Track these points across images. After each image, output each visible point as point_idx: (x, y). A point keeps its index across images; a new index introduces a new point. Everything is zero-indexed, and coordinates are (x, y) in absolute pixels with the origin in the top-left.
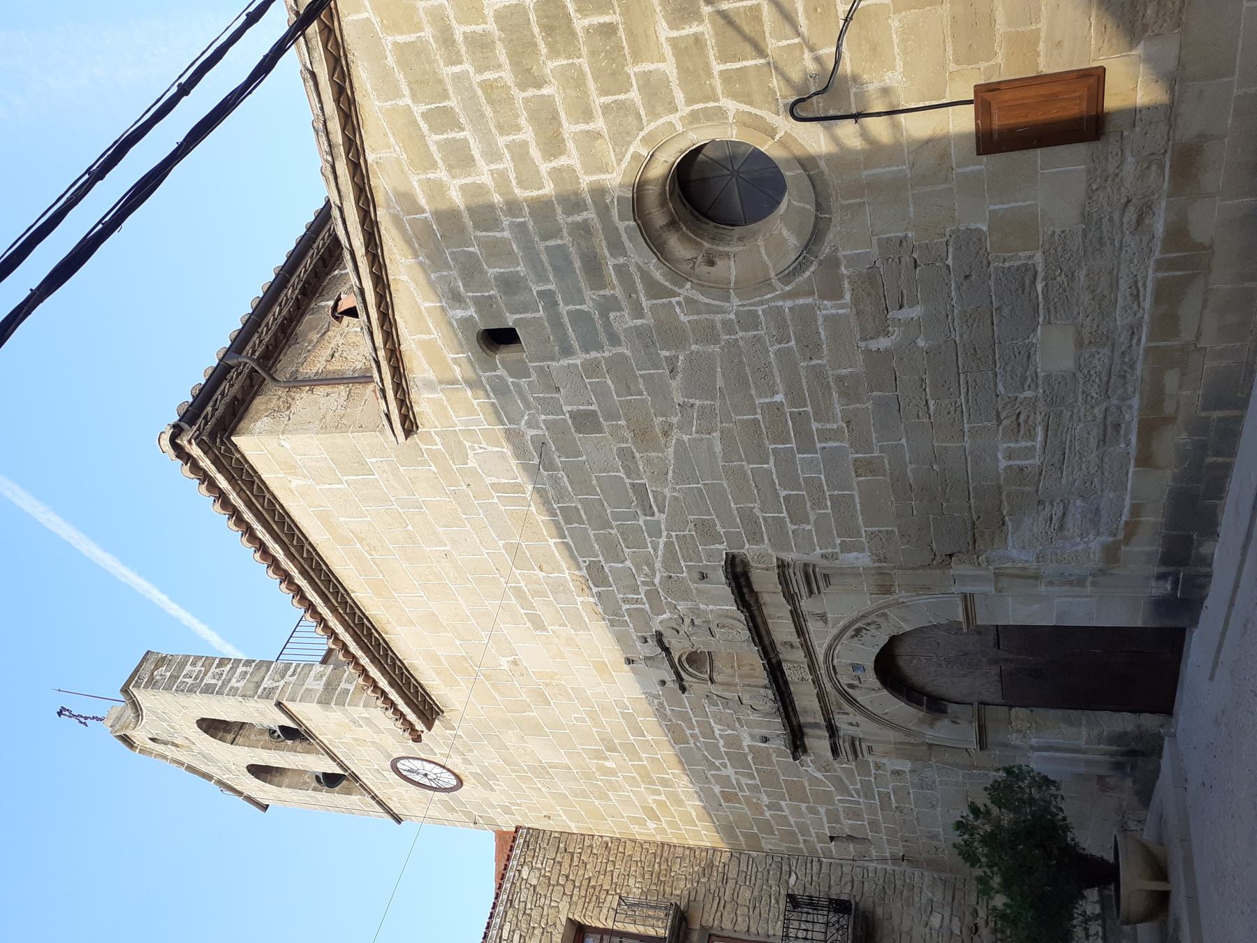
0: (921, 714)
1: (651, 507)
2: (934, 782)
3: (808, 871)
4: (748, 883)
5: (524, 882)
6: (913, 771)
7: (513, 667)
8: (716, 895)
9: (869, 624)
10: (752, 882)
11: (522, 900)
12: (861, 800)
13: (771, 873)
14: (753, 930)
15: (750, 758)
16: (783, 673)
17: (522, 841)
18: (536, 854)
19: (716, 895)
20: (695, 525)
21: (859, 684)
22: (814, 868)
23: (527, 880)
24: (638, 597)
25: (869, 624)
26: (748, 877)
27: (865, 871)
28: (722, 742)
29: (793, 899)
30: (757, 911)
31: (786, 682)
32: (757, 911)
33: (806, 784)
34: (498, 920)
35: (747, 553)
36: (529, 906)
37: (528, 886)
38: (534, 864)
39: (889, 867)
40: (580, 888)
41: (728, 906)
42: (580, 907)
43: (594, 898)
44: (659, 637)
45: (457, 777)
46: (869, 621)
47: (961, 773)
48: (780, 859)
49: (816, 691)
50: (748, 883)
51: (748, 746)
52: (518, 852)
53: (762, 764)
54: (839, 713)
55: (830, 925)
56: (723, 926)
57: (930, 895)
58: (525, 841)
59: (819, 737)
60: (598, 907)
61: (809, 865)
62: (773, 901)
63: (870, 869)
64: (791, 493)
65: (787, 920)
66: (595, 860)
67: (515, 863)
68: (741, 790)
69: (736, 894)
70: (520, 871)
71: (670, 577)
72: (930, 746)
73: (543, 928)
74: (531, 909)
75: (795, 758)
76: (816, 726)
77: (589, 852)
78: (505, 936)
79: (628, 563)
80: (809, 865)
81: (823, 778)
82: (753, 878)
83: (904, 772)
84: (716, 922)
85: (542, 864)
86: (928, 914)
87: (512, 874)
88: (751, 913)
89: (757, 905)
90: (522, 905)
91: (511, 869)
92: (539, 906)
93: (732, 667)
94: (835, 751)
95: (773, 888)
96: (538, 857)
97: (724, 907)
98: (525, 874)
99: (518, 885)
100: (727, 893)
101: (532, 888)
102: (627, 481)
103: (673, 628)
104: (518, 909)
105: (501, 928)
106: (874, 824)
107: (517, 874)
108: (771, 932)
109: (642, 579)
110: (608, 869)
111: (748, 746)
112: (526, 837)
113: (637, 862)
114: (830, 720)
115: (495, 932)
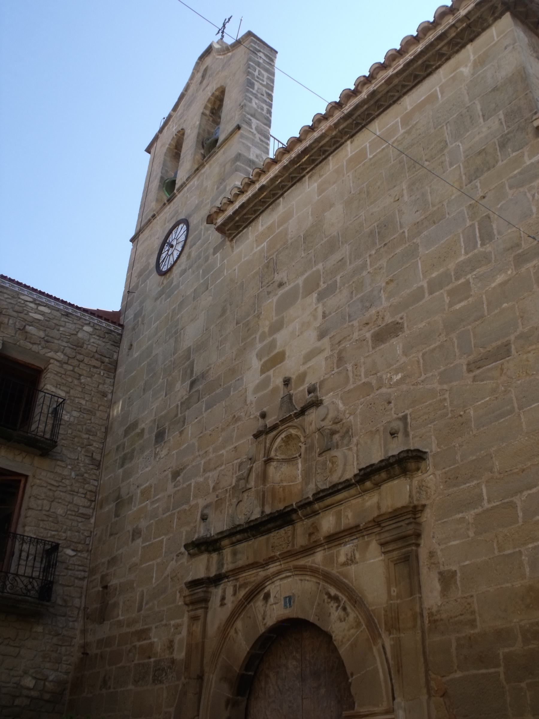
0: (237, 669)
1: (479, 368)
2: (161, 682)
3: (76, 567)
4: (69, 512)
5: (80, 327)
6: (173, 661)
7: (276, 284)
8: (61, 484)
9: (344, 609)
10: (70, 517)
11: (67, 324)
12: (142, 612)
13: (77, 534)
14: (30, 513)
15: (186, 507)
16: (280, 527)
17: (112, 328)
18: (101, 339)
19: (61, 484)
20: (461, 416)
21: (269, 603)
22: (79, 573)
23: (82, 329)
24: (363, 376)
25: (344, 609)
26: (74, 513)
27: (74, 619)
28: (201, 479)
29: (55, 547)
30: (45, 518)
31: (269, 531)
32: (45, 518)
33: (159, 560)
34: (53, 304)
35: (429, 473)
36: (62, 329)
37: (77, 330)
38: (94, 336)
39: (78, 641)
40: (73, 371)
41: (51, 494)
42: (58, 370)
43: (64, 382)
44: (316, 403)
45: (170, 270)
46: (349, 610)
47: (172, 710)
48: (87, 542)
49: (261, 561)
50: (69, 512)
51: (197, 504)
52: (104, 325)
53: (179, 519)
54: (235, 586)
55: (31, 580)
56: (34, 487)
57: (51, 678)
58: (111, 330)
59: (208, 568)
60: (57, 384)
61: (81, 568)
62: (53, 533)
63: (76, 624)
64: (519, 509)
65: (38, 541)
66: (94, 385)
67: (96, 322)
68: (153, 503)
69: (60, 501)
70: (89, 324)
71: (390, 403)
72: (200, 678)
73: (43, 338)
74: (58, 330)
75: (186, 546)
76: (221, 564)
77: (101, 381)
78: (41, 308)
79: (404, 359)
80: (81, 568)
81: (165, 575)
82: (73, 517)
83: (172, 653)
84: (38, 481)
85: (93, 342)
86: (34, 675)
87: (87, 318)
88: (44, 512)
89: (51, 519)
90: (63, 324)
91: (92, 318)
92: (61, 337)
93: (282, 481)
94: (194, 584)
95: (64, 535)
96: (99, 340)
97: (50, 490)
98: (87, 328)
99: (78, 322)
100: (61, 494)
101: (76, 333)
102: (512, 338)
103: (327, 414)
104: (60, 320)
105: (46, 306)
106: (120, 624)
107: (87, 322)
108: (27, 529)
109: (384, 377)
110: (86, 395)
111: (197, 504)
112: (114, 332)
113: (90, 420)
114: (227, 577)
115: (44, 300)
